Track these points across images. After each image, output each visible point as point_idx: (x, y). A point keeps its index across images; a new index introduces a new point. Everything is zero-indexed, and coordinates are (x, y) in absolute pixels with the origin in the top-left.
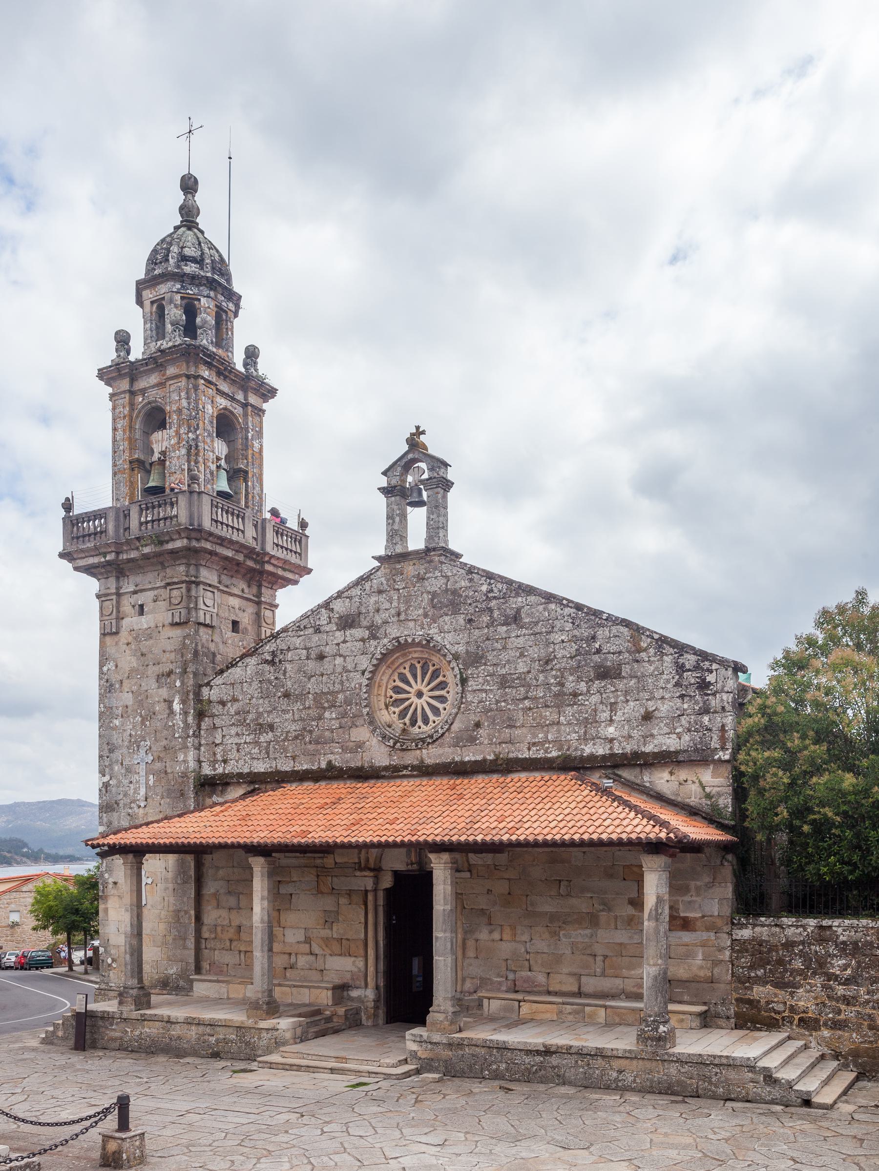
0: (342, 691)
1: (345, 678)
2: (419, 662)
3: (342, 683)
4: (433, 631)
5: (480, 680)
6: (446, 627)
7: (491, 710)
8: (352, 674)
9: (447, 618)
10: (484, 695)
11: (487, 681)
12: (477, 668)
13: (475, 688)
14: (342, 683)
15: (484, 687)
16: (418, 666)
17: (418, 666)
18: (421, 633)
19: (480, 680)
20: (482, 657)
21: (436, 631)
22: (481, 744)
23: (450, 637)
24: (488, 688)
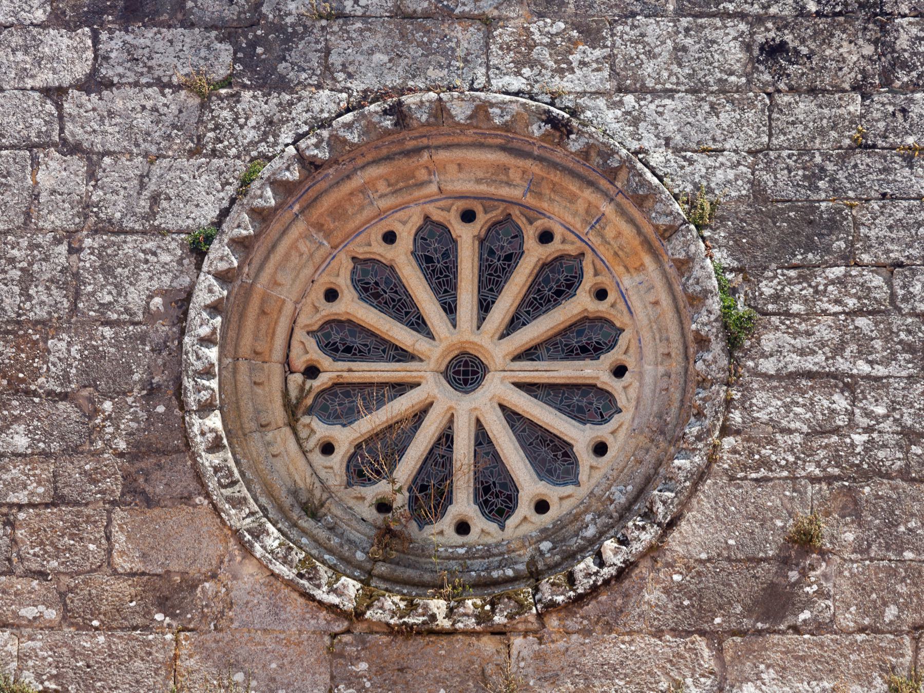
0: (73, 320)
1: (88, 260)
2: (468, 216)
3: (72, 282)
4: (579, 78)
5: (824, 330)
6: (649, 68)
7: (878, 473)
8: (130, 246)
9: (653, 29)
10: (841, 402)
11: (858, 336)
12: (806, 272)
13: (795, 362)
14: (72, 282)
15: (842, 364)
16: (467, 237)
17: (467, 237)
18: (517, 84)
19: (824, 330)
20: (833, 224)
21: (598, 79)
22: (818, 627)
23: (670, 114)
24: (863, 367)
